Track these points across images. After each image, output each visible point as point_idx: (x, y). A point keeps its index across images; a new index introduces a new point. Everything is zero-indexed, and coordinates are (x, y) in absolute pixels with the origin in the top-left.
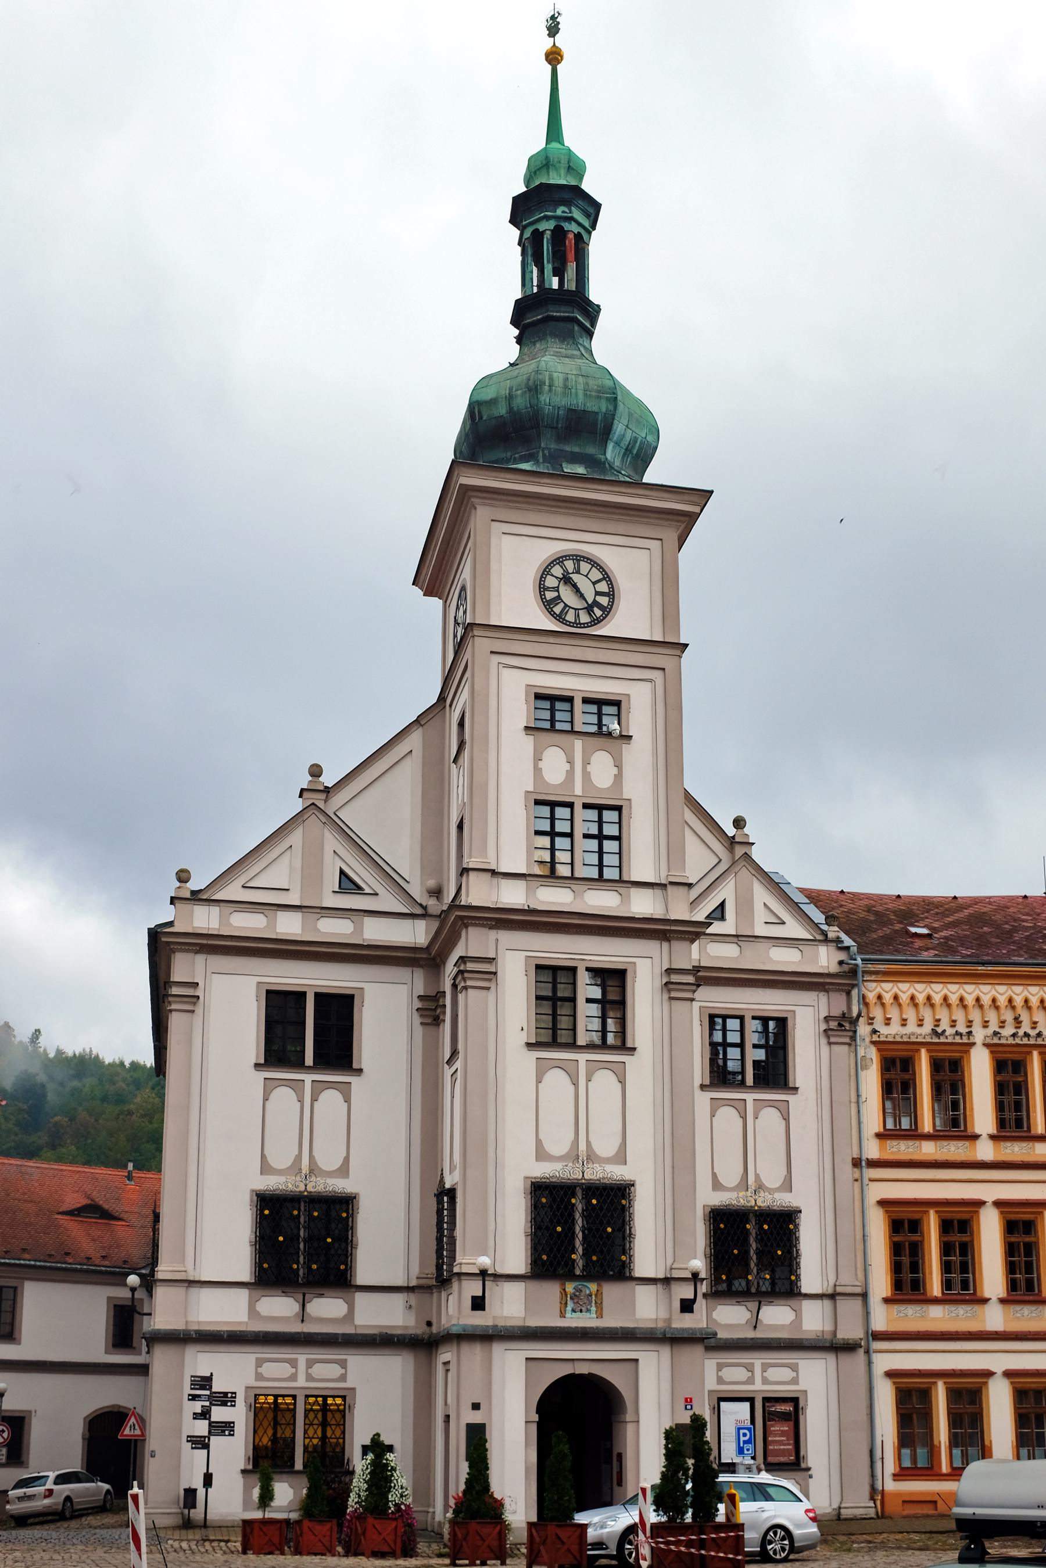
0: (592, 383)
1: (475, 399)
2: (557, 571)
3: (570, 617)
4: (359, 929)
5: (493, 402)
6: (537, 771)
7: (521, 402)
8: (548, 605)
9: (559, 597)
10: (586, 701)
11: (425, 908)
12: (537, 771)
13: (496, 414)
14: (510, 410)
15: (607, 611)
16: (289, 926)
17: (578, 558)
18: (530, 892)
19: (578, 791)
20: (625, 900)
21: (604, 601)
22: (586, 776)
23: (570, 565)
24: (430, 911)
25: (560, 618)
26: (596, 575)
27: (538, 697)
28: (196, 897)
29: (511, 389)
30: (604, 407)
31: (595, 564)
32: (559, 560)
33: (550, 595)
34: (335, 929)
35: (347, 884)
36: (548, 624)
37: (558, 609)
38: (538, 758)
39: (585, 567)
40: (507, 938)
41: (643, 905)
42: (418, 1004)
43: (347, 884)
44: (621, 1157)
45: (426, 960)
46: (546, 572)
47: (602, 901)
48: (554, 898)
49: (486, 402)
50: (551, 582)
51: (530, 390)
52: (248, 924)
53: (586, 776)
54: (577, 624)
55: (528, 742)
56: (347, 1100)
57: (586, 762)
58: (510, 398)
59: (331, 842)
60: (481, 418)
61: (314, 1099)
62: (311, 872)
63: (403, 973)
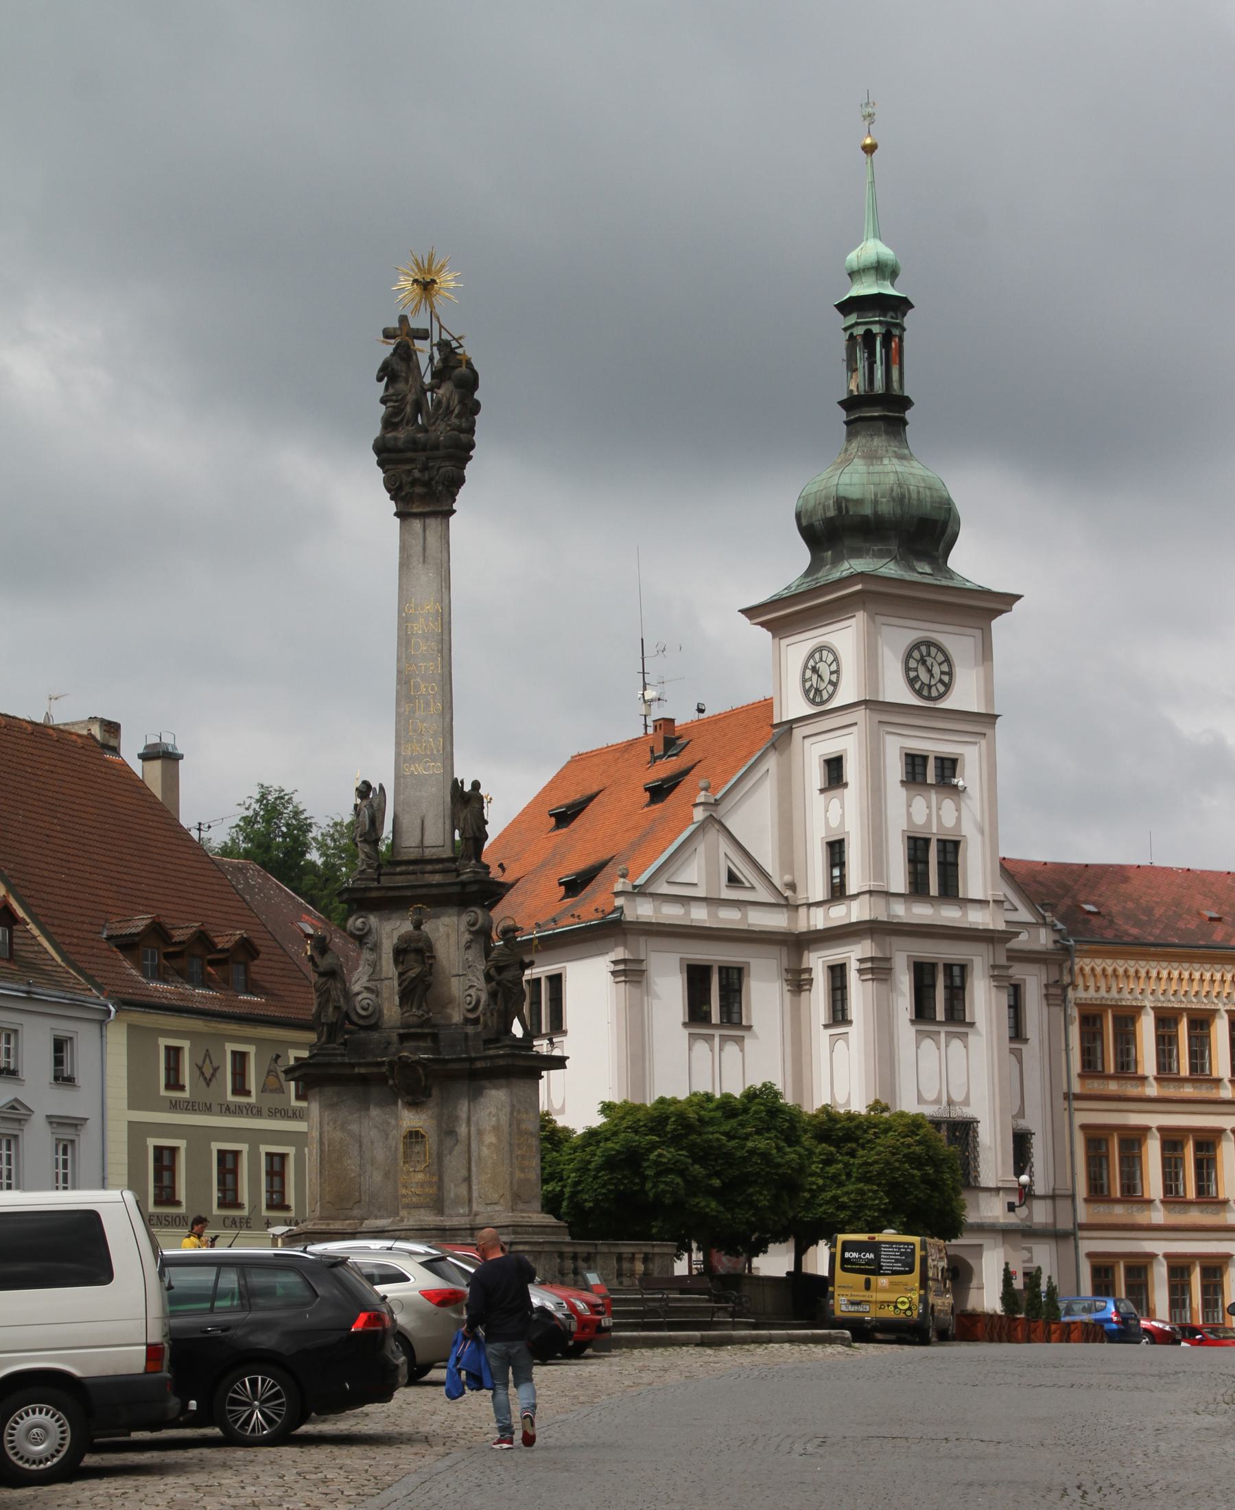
0: (935, 494)
1: (842, 493)
2: (916, 654)
3: (925, 693)
4: (745, 917)
5: (859, 502)
6: (909, 815)
7: (886, 508)
8: (912, 682)
9: (917, 676)
10: (936, 758)
11: (786, 898)
12: (909, 815)
13: (862, 513)
14: (876, 513)
15: (948, 686)
16: (699, 915)
17: (929, 644)
18: (908, 909)
19: (934, 830)
20: (965, 915)
21: (946, 678)
22: (939, 817)
23: (924, 649)
24: (791, 902)
25: (919, 693)
26: (940, 658)
27: (907, 755)
28: (639, 892)
29: (876, 495)
30: (942, 516)
31: (940, 649)
32: (916, 646)
33: (912, 674)
34: (729, 918)
35: (733, 879)
36: (914, 701)
37: (917, 686)
38: (909, 806)
39: (933, 651)
40: (897, 942)
41: (978, 918)
42: (785, 975)
43: (733, 879)
44: (966, 1102)
45: (798, 944)
46: (909, 656)
47: (949, 915)
48: (922, 913)
49: (853, 500)
50: (913, 664)
51: (894, 500)
52: (671, 913)
53: (939, 817)
54: (929, 698)
55: (902, 793)
56: (742, 1050)
57: (939, 809)
58: (875, 502)
59: (724, 846)
60: (847, 511)
61: (721, 1050)
62: (711, 873)
63: (775, 950)
